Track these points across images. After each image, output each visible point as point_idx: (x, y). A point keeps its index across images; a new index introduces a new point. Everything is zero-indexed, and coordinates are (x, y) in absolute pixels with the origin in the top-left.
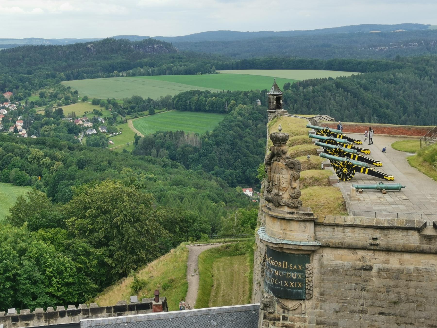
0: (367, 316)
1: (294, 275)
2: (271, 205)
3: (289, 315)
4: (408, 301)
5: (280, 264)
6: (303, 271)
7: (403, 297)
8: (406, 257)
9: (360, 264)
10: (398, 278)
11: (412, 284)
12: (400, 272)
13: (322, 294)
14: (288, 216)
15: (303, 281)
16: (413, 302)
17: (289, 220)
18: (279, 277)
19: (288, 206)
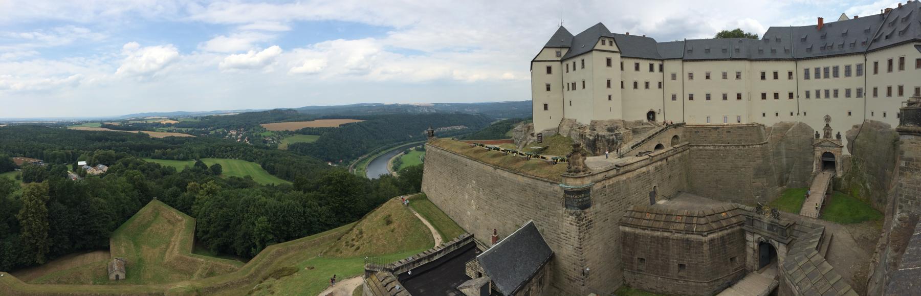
0: (608, 204)
1: (587, 198)
2: (572, 173)
3: (587, 215)
4: (616, 193)
5: (581, 196)
6: (589, 196)
7: (615, 193)
8: (614, 179)
9: (603, 186)
10: (613, 187)
11: (616, 187)
12: (613, 184)
13: (595, 202)
14: (584, 175)
15: (589, 199)
16: (618, 192)
17: (584, 177)
18: (581, 202)
19: (583, 171)
